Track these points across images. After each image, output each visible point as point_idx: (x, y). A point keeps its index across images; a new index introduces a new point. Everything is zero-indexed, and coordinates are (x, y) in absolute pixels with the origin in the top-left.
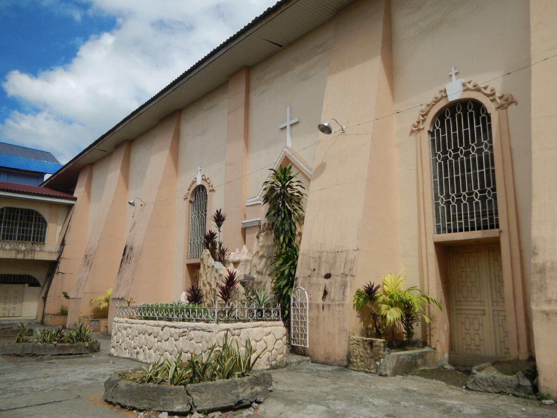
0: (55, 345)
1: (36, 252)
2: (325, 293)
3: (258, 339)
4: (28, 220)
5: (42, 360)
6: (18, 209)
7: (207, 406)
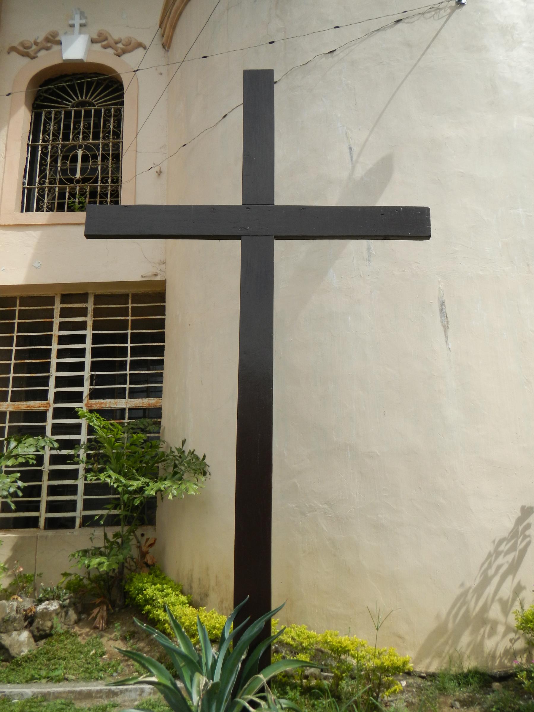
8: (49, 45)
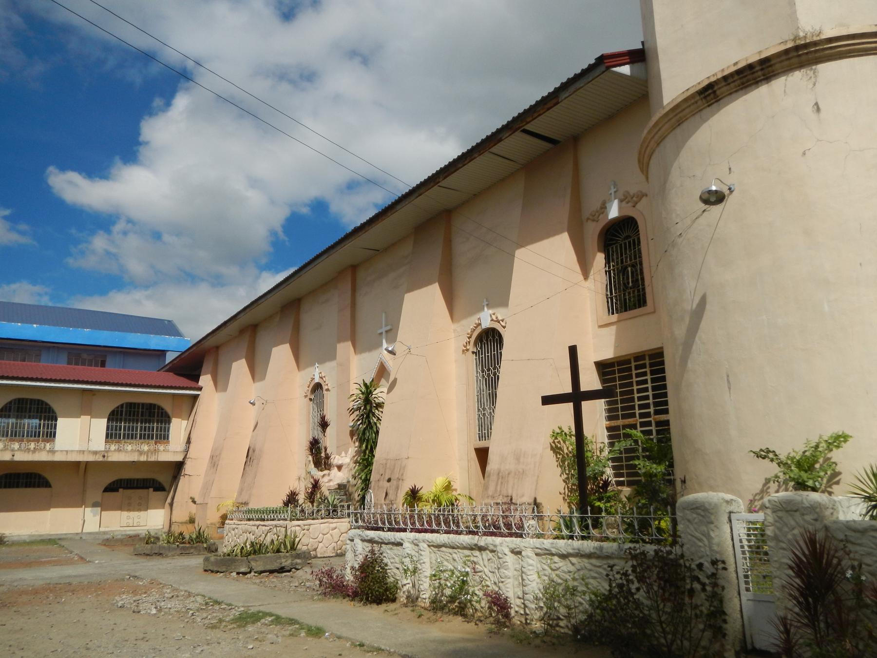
0: (178, 545)
1: (160, 453)
2: (387, 494)
3: (325, 533)
4: (150, 416)
5: (167, 556)
6: (139, 404)
7: (260, 569)
8: (603, 210)
